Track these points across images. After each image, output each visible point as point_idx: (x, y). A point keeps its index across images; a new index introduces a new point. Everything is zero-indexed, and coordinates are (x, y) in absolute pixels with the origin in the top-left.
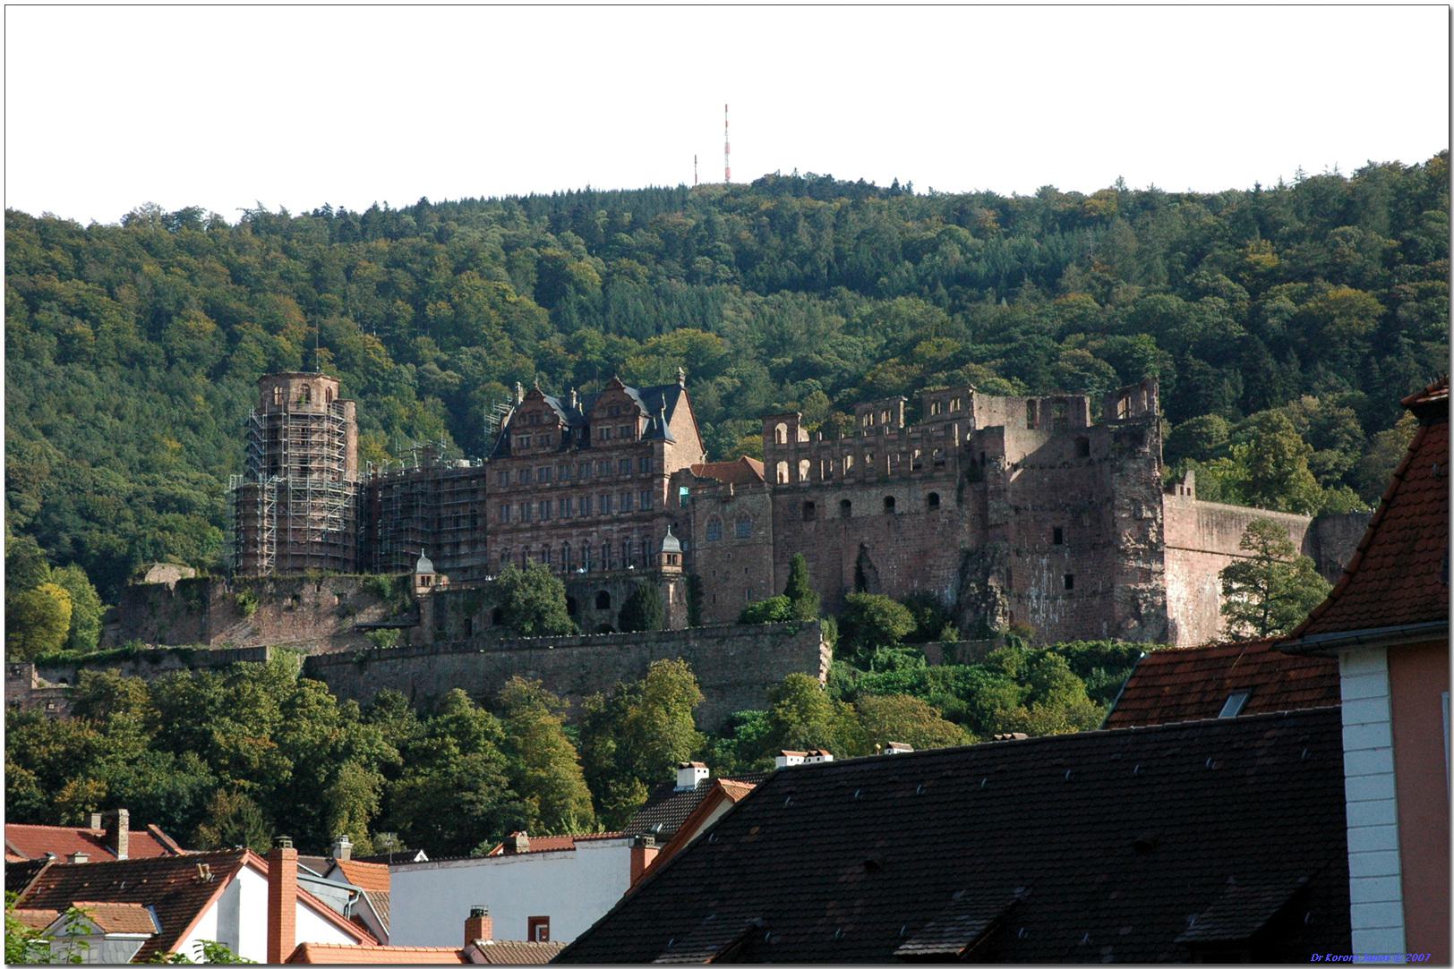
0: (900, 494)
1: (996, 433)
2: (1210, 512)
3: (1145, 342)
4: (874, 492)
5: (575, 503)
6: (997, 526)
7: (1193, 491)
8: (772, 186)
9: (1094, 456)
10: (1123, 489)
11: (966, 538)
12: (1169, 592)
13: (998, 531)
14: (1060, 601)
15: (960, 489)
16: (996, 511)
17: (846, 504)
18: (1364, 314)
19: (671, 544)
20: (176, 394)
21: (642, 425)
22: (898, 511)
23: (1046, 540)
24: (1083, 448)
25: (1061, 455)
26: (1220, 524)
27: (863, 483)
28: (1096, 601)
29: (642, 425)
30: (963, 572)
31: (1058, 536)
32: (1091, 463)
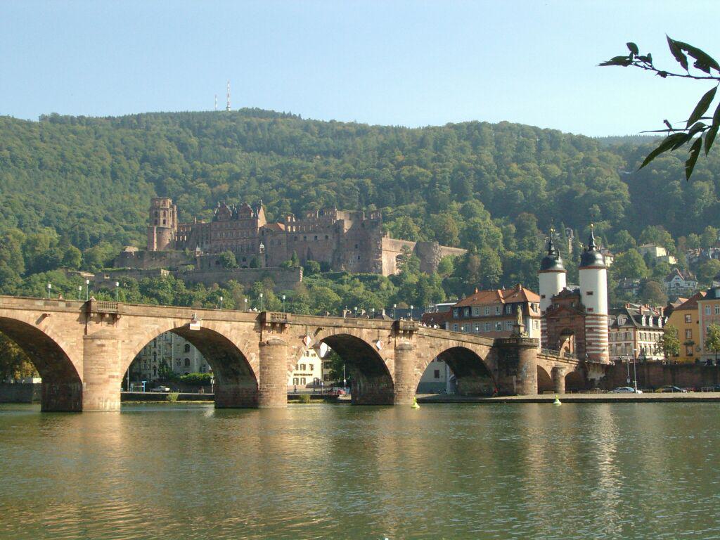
1: (342, 221)
3: (368, 181)
5: (234, 233)
8: (245, 112)
9: (366, 227)
15: (333, 234)
17: (305, 237)
18: (427, 177)
19: (262, 246)
20: (77, 181)
21: (252, 215)
23: (354, 247)
24: (363, 225)
26: (394, 245)
27: (310, 232)
29: (252, 215)
30: (333, 255)
31: (356, 246)
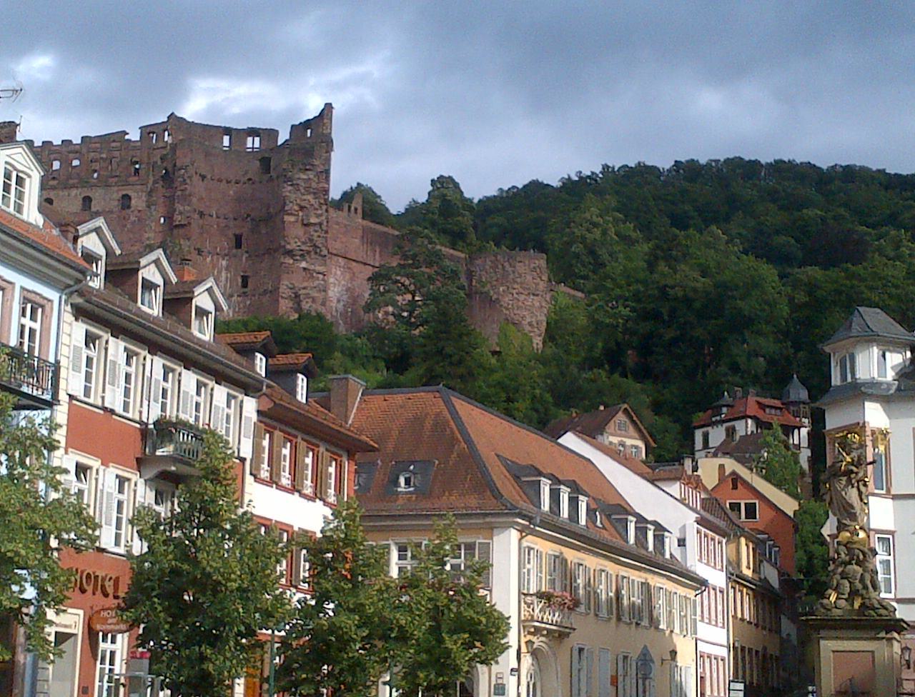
0: (97, 195)
2: (373, 231)
4: (74, 192)
6: (182, 226)
7: (360, 211)
9: (273, 174)
10: (293, 196)
11: (152, 235)
12: (330, 293)
13: (181, 231)
14: (235, 298)
15: (150, 194)
16: (181, 213)
22: (93, 209)
23: (226, 244)
25: (246, 173)
28: (266, 299)
32: (271, 179)
